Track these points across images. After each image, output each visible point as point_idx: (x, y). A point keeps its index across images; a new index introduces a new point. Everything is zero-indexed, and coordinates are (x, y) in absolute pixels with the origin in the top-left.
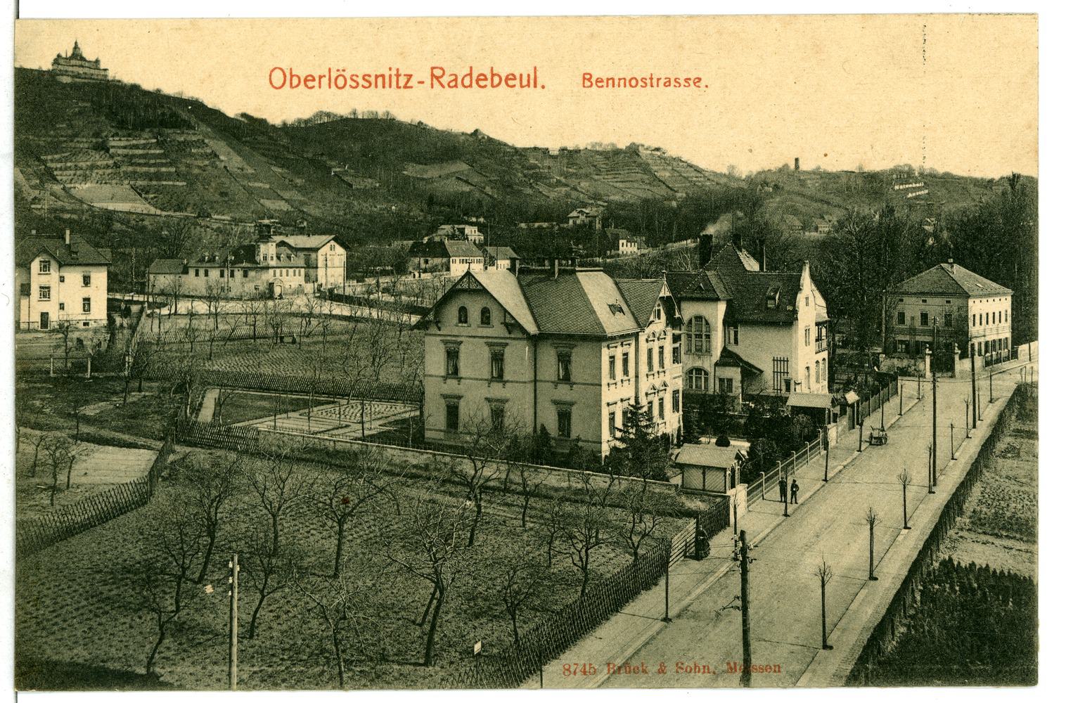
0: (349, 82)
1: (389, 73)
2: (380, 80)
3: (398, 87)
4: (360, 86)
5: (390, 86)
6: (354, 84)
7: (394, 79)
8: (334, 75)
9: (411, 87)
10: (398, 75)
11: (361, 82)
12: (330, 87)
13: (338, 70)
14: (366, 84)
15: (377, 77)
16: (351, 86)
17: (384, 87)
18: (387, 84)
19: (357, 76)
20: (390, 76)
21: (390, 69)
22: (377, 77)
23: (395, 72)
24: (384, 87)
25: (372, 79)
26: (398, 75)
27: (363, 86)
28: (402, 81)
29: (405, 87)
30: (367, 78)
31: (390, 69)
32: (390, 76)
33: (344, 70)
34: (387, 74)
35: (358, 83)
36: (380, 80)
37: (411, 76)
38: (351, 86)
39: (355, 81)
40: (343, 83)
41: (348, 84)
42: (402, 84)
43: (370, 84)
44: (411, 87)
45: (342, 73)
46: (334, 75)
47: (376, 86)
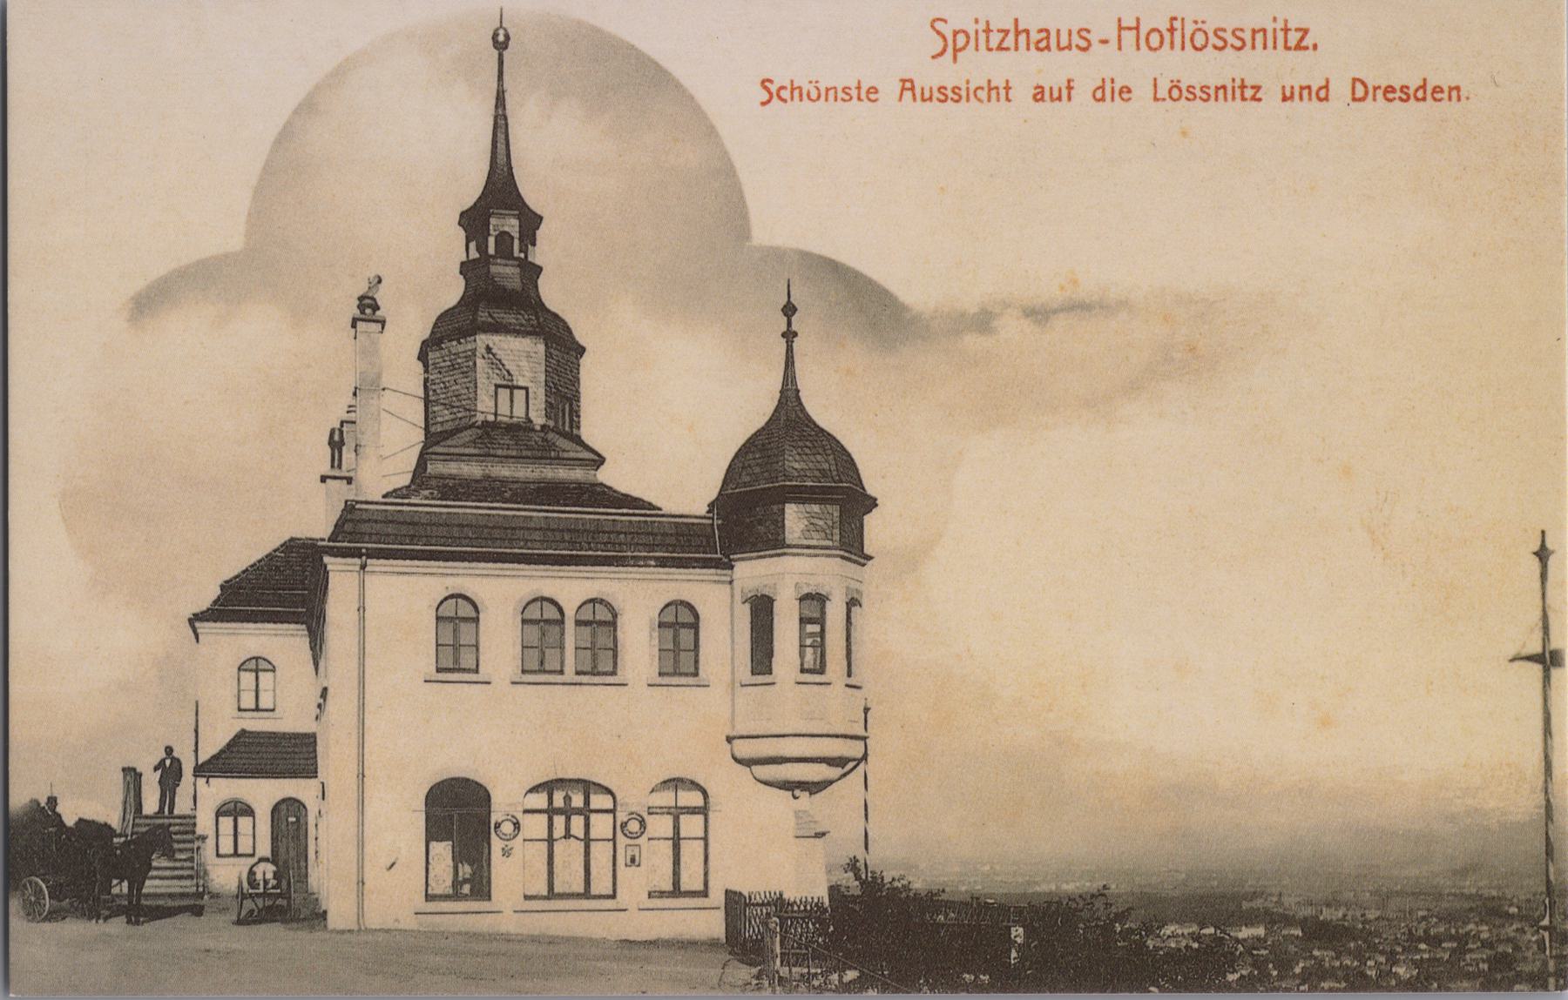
0: (1213, 40)
1: (1274, 25)
2: (1259, 36)
3: (1287, 48)
4: (1229, 46)
5: (1275, 48)
6: (1220, 44)
7: (1280, 35)
8: (1189, 29)
9: (1306, 48)
10: (1286, 30)
11: (1231, 40)
12: (1183, 48)
13: (1196, 22)
14: (1239, 44)
15: (1254, 32)
16: (1215, 47)
17: (1265, 47)
18: (1270, 43)
19: (1224, 30)
20: (1275, 30)
21: (1275, 19)
22: (1254, 32)
23: (1283, 27)
24: (1265, 47)
25: (1247, 36)
26: (1286, 30)
27: (1232, 46)
28: (1294, 38)
29: (1296, 49)
30: (1239, 33)
31: (1275, 19)
32: (1275, 30)
33: (1203, 22)
34: (1270, 27)
35: (1225, 41)
36: (1259, 36)
37: (1306, 32)
38: (1215, 47)
39: (1220, 38)
40: (1203, 43)
41: (1210, 48)
42: (1292, 42)
43: (1244, 44)
44: (1306, 48)
45: (1204, 27)
46: (1189, 29)
47: (1254, 47)
